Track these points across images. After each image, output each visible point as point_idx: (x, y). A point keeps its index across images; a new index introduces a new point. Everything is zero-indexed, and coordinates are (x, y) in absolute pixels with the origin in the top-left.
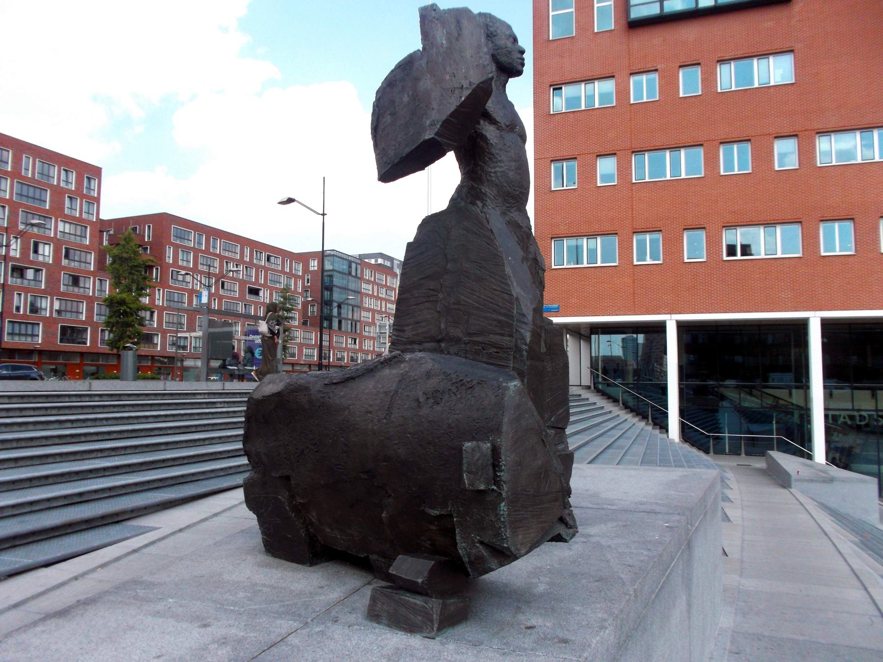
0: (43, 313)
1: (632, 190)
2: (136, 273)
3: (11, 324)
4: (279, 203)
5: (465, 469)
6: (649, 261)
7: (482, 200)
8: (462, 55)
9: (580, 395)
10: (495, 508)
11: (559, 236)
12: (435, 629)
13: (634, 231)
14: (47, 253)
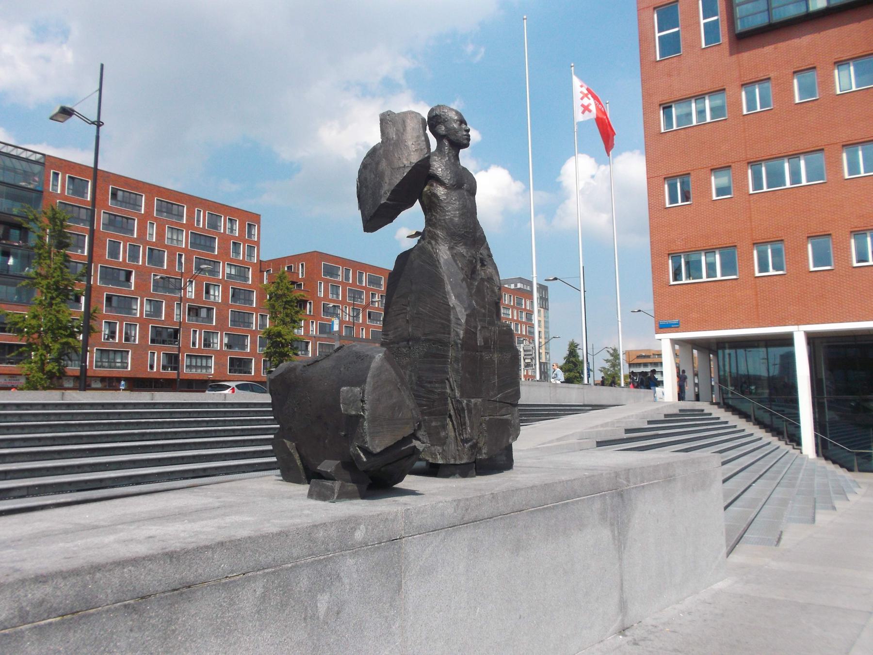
0: (215, 345)
1: (749, 201)
2: (290, 307)
4: (408, 237)
5: (341, 401)
6: (772, 272)
7: (436, 241)
9: (703, 410)
10: (363, 424)
11: (676, 252)
12: (335, 497)
13: (755, 242)
14: (217, 294)
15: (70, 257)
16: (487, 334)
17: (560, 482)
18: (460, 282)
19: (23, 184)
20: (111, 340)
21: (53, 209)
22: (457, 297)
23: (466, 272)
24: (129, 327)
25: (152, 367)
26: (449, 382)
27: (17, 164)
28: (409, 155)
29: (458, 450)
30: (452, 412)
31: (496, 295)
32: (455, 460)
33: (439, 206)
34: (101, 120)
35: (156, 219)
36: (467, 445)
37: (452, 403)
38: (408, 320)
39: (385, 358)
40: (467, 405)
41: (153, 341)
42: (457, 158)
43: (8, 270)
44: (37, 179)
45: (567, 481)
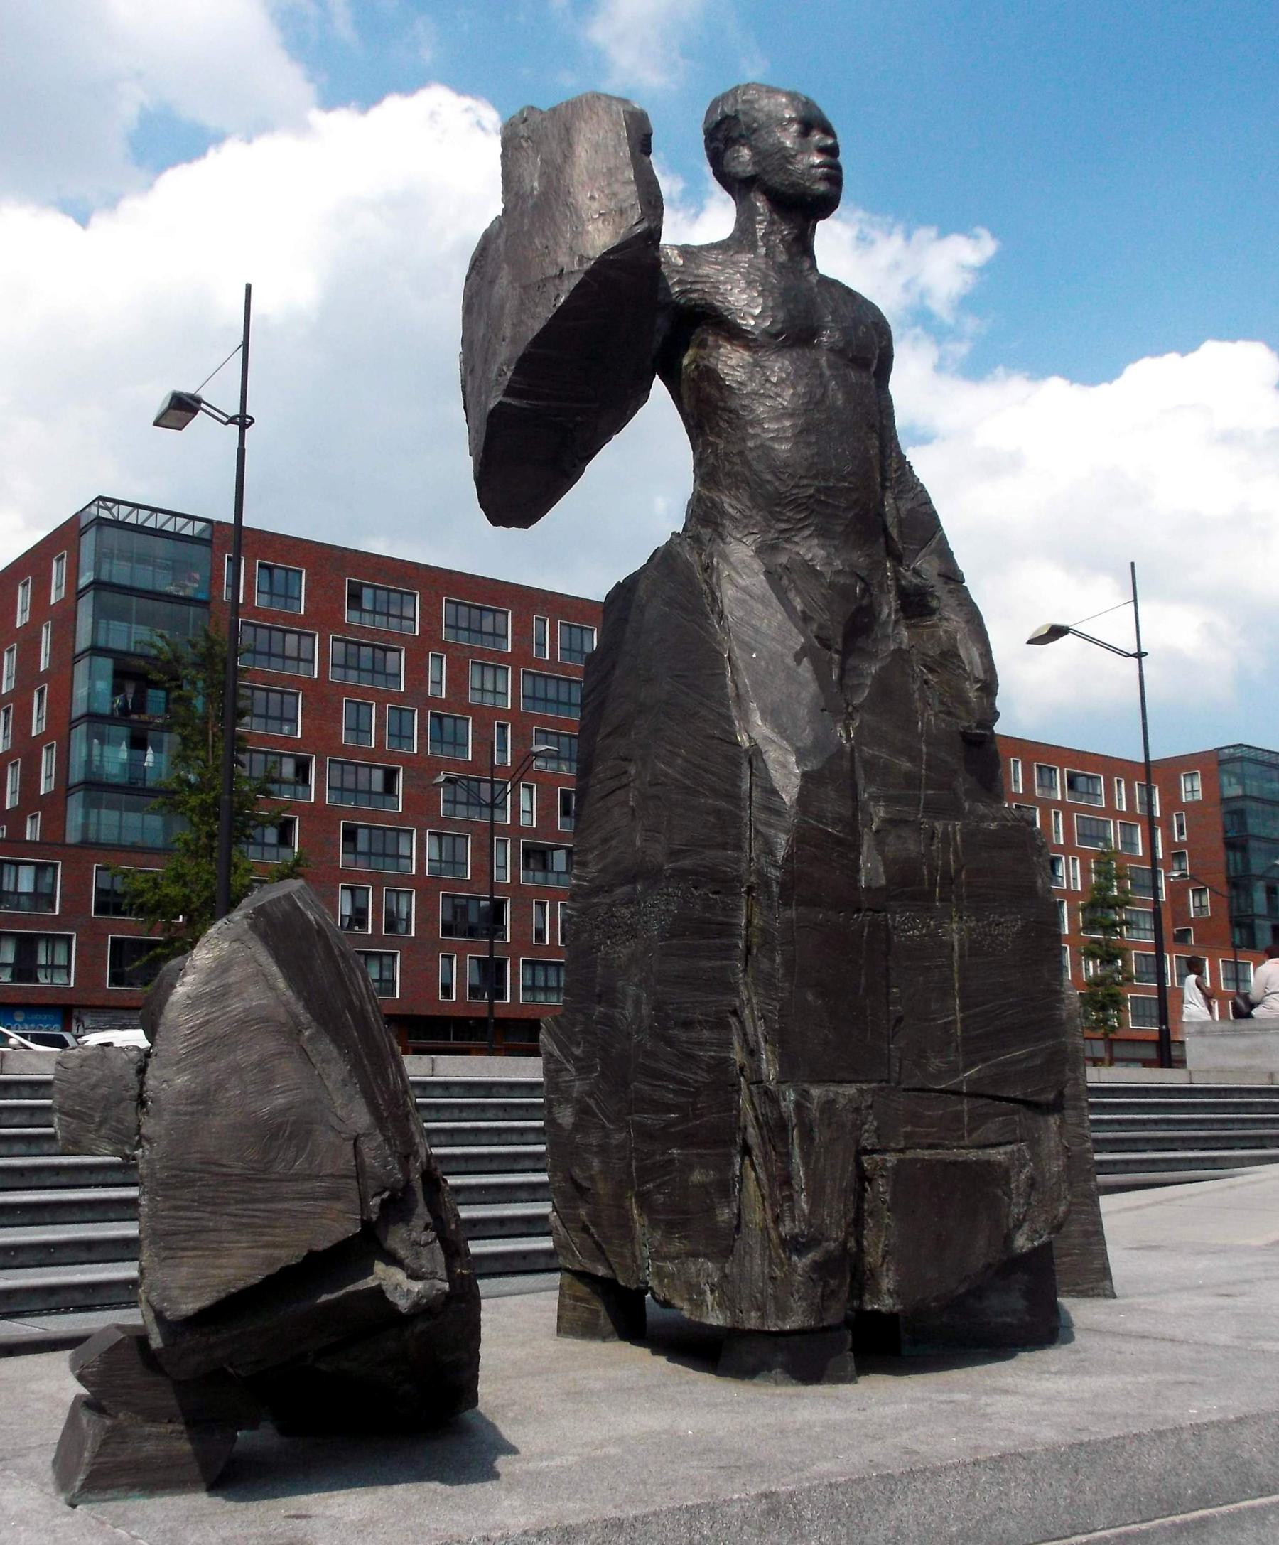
3: (528, 967)
4: (1030, 642)
8: (571, 200)
15: (247, 741)
16: (912, 847)
17: (1161, 1434)
18: (790, 661)
19: (171, 589)
20: (357, 928)
21: (207, 637)
22: (771, 715)
23: (821, 627)
24: (394, 895)
25: (447, 990)
26: (741, 1022)
27: (161, 545)
28: (579, 233)
29: (773, 1279)
30: (753, 1135)
31: (969, 712)
32: (763, 1317)
33: (724, 409)
34: (247, 413)
35: (445, 646)
36: (802, 1263)
37: (753, 1104)
38: (633, 809)
39: (253, 927)
40: (799, 1106)
41: (448, 930)
42: (803, 246)
43: (145, 780)
44: (197, 576)
45: (1198, 1430)
